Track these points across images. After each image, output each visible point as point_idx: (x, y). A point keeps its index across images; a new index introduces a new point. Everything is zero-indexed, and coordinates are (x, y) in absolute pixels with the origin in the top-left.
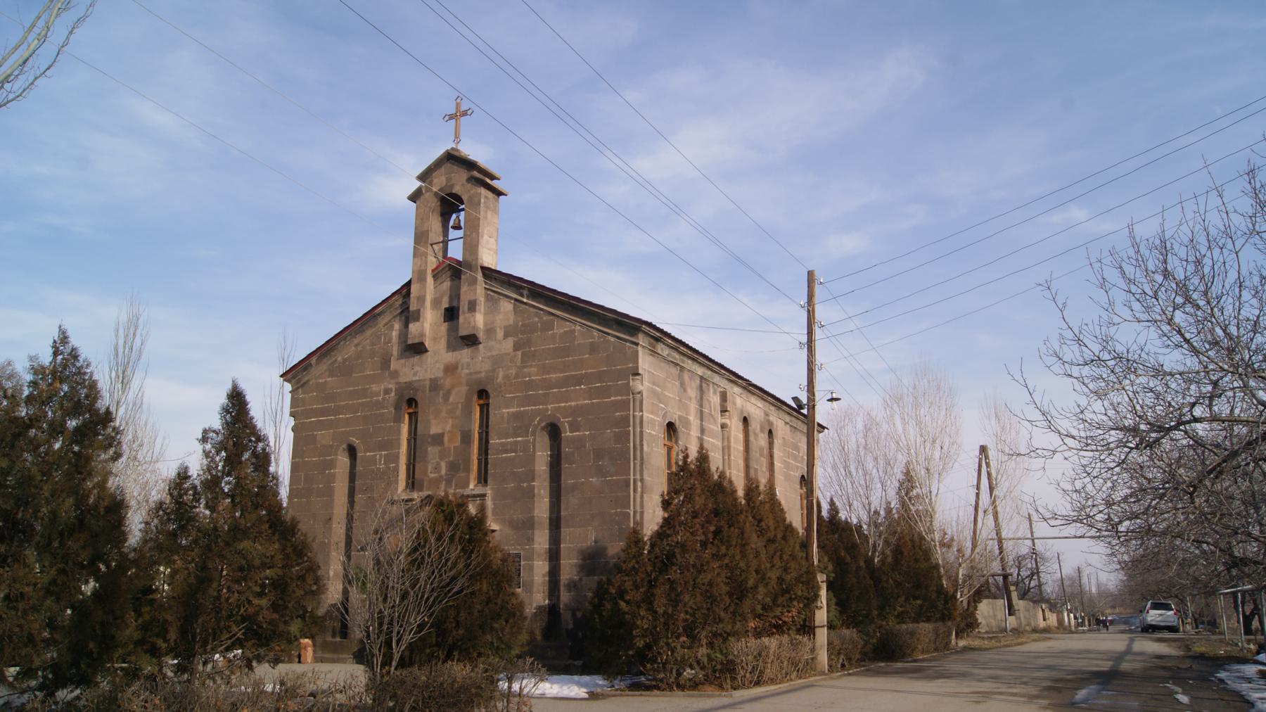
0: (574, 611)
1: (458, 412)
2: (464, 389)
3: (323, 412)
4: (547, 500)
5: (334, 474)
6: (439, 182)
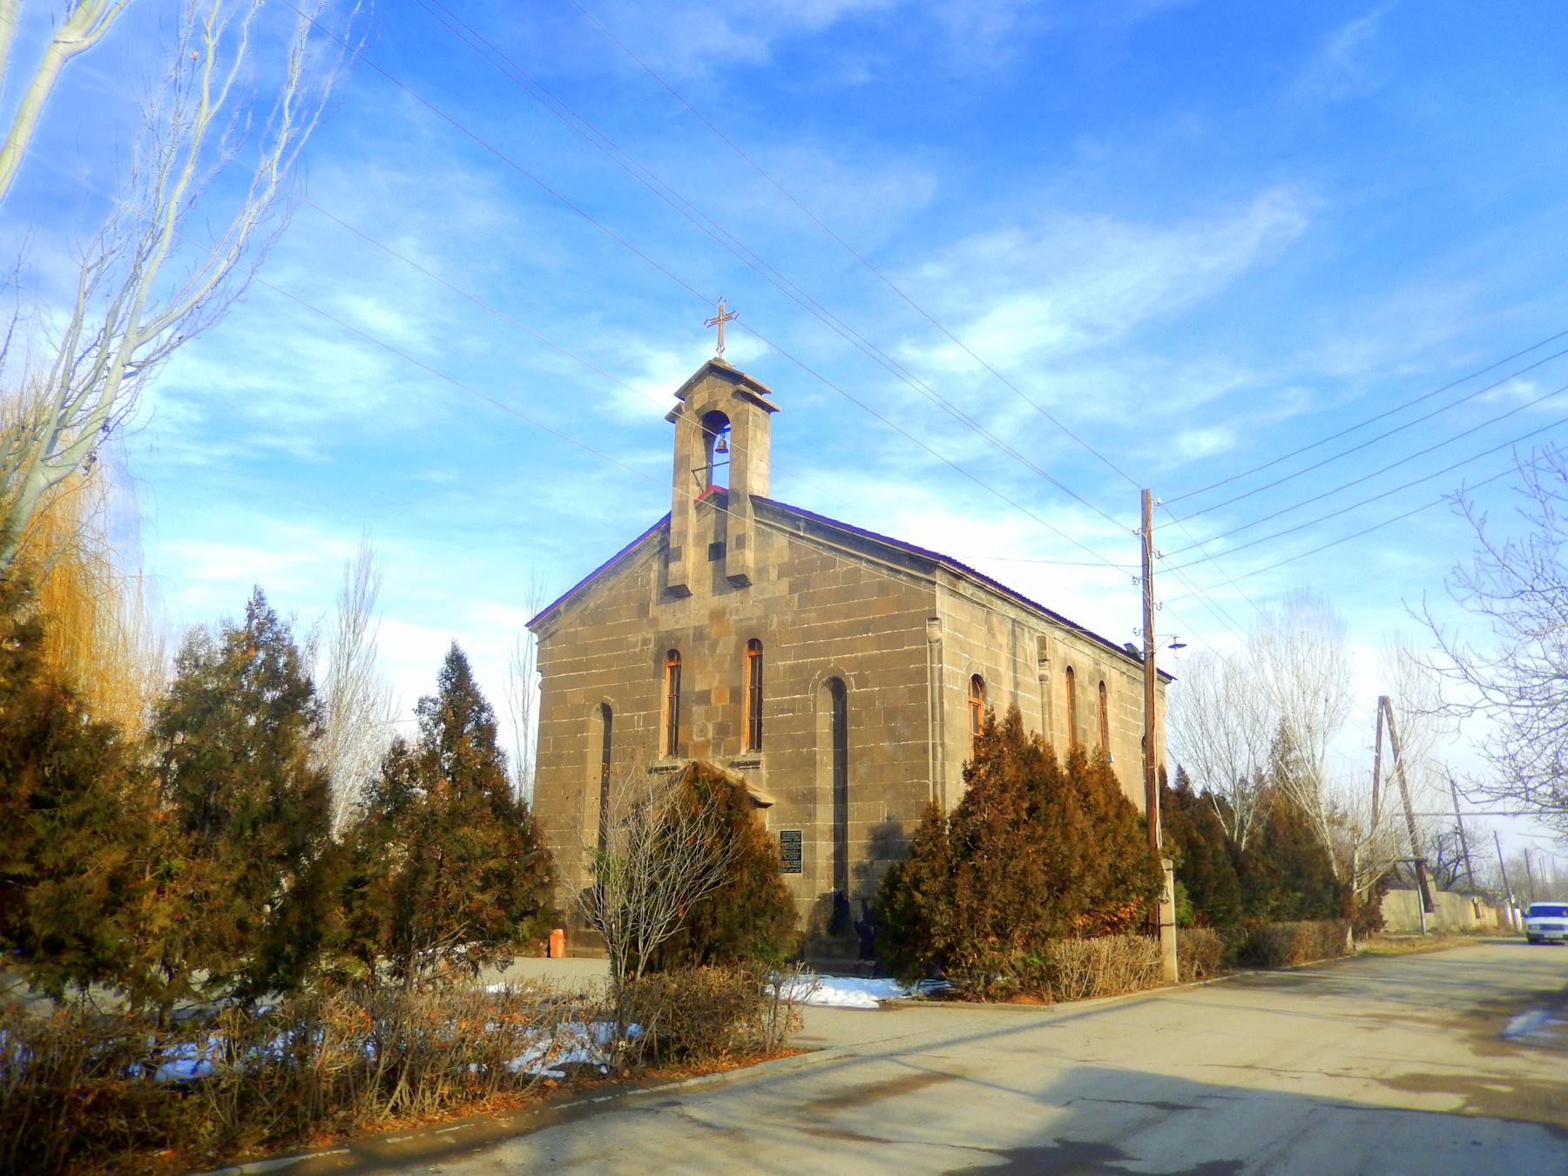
0: (864, 901)
1: (727, 666)
2: (733, 638)
3: (574, 666)
4: (831, 768)
5: (587, 738)
6: (701, 398)
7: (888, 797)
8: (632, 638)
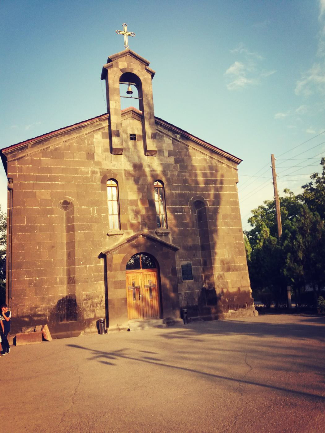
6: (123, 64)
7: (228, 247)
8: (84, 169)
